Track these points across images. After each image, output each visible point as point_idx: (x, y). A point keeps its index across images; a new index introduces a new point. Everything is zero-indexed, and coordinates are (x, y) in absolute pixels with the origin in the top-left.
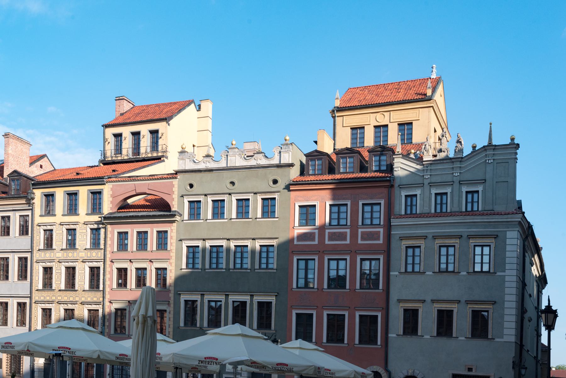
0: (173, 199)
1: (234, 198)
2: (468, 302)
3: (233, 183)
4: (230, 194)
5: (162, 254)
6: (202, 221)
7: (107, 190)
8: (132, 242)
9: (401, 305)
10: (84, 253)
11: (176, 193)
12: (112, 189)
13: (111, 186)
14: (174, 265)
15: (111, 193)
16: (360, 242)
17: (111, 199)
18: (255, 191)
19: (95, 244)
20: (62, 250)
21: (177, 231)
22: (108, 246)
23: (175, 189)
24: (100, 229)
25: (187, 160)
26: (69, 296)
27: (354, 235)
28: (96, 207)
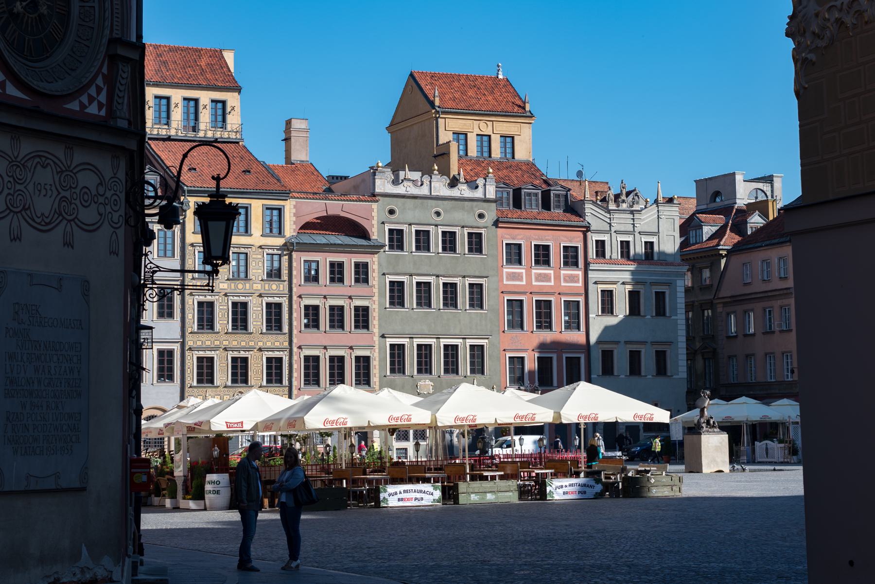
2: (653, 343)
5: (361, 289)
7: (289, 207)
9: (601, 346)
10: (259, 286)
11: (375, 218)
12: (295, 207)
13: (294, 203)
14: (377, 303)
15: (294, 211)
16: (563, 284)
17: (294, 219)
18: (463, 224)
19: (274, 274)
20: (228, 280)
21: (380, 265)
23: (375, 214)
26: (239, 340)
27: (557, 277)
28: (275, 225)
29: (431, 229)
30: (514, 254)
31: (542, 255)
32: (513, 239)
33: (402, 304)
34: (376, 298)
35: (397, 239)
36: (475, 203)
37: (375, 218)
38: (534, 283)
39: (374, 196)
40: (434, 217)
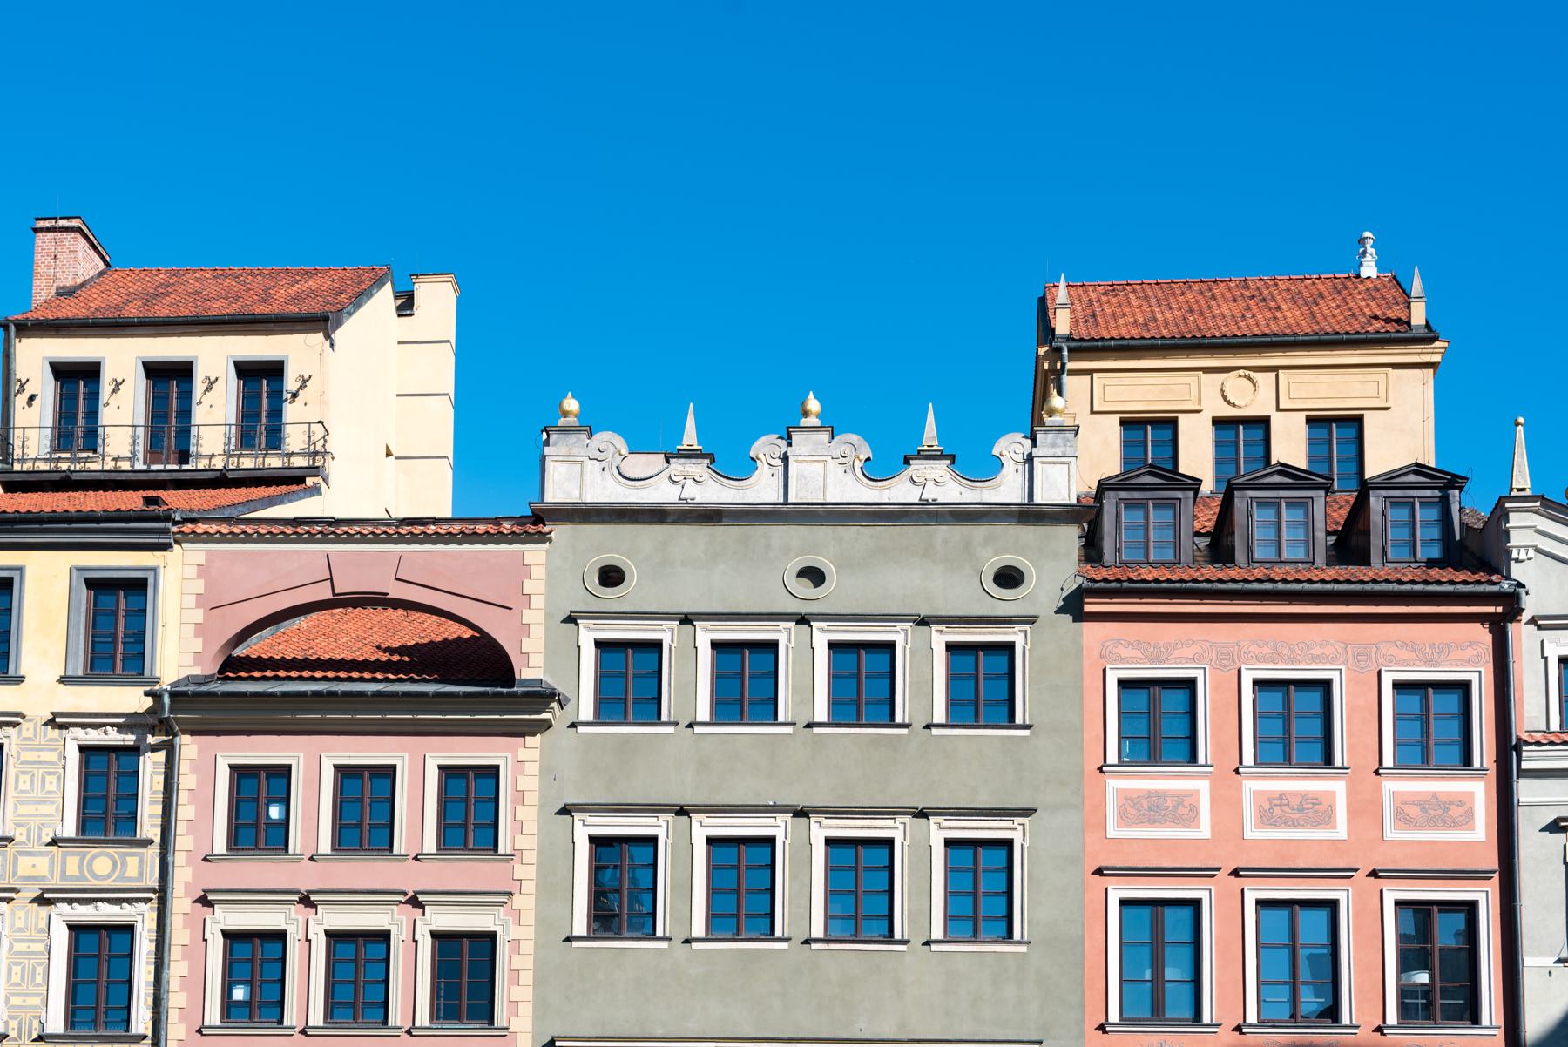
0: (525, 629)
1: (822, 636)
3: (814, 575)
4: (803, 620)
6: (670, 729)
8: (312, 812)
10: (46, 860)
11: (538, 602)
12: (203, 571)
13: (200, 558)
14: (529, 918)
15: (199, 586)
16: (1391, 834)
21: (548, 773)
22: (181, 828)
23: (535, 586)
24: (135, 751)
25: (589, 464)
29: (783, 634)
30: (1160, 720)
31: (1297, 722)
32: (1156, 660)
33: (645, 925)
34: (525, 901)
35: (631, 679)
36: (979, 531)
37: (538, 602)
38: (1250, 833)
39: (537, 521)
40: (805, 588)
